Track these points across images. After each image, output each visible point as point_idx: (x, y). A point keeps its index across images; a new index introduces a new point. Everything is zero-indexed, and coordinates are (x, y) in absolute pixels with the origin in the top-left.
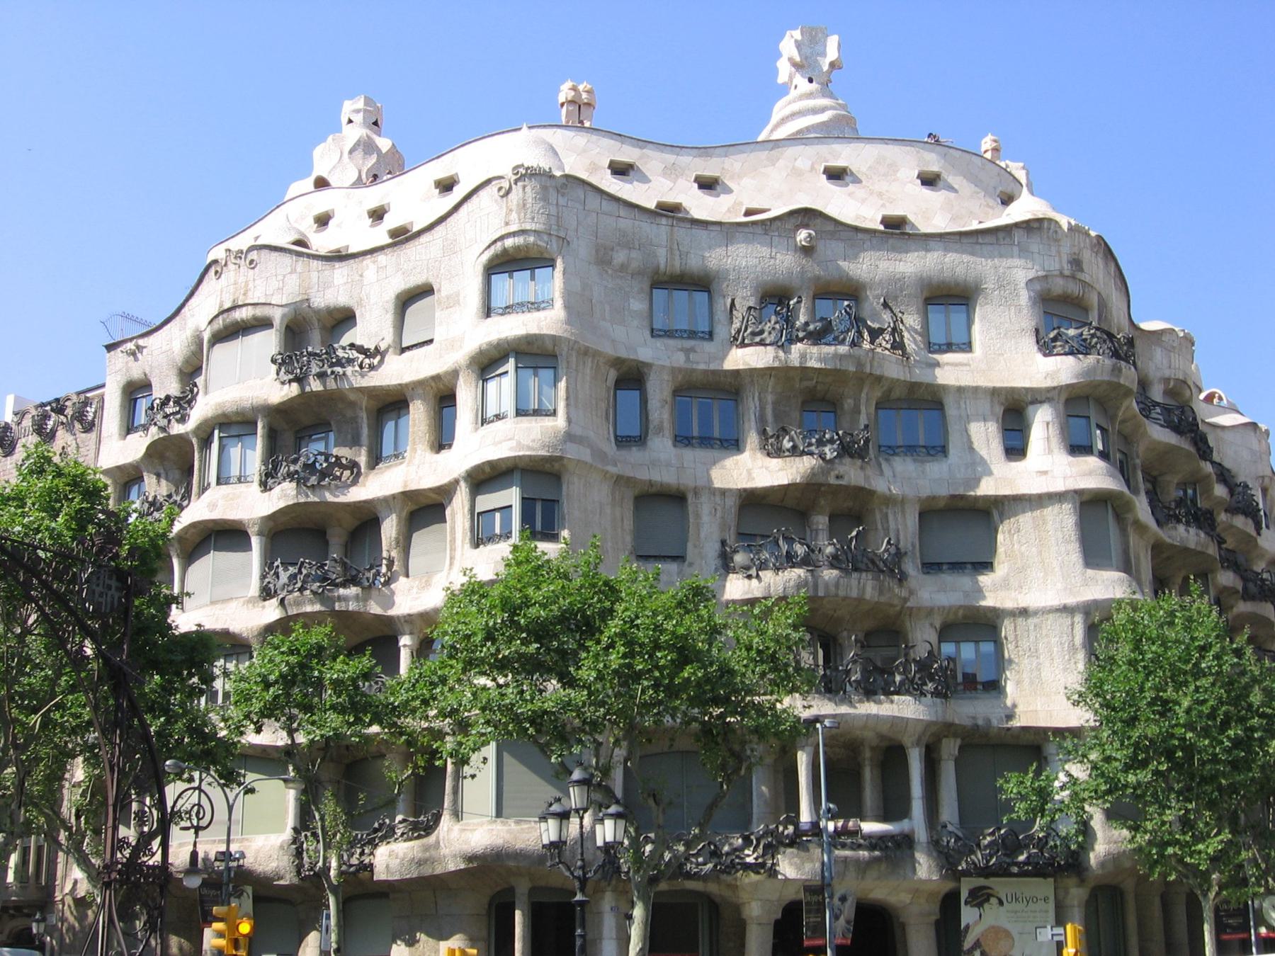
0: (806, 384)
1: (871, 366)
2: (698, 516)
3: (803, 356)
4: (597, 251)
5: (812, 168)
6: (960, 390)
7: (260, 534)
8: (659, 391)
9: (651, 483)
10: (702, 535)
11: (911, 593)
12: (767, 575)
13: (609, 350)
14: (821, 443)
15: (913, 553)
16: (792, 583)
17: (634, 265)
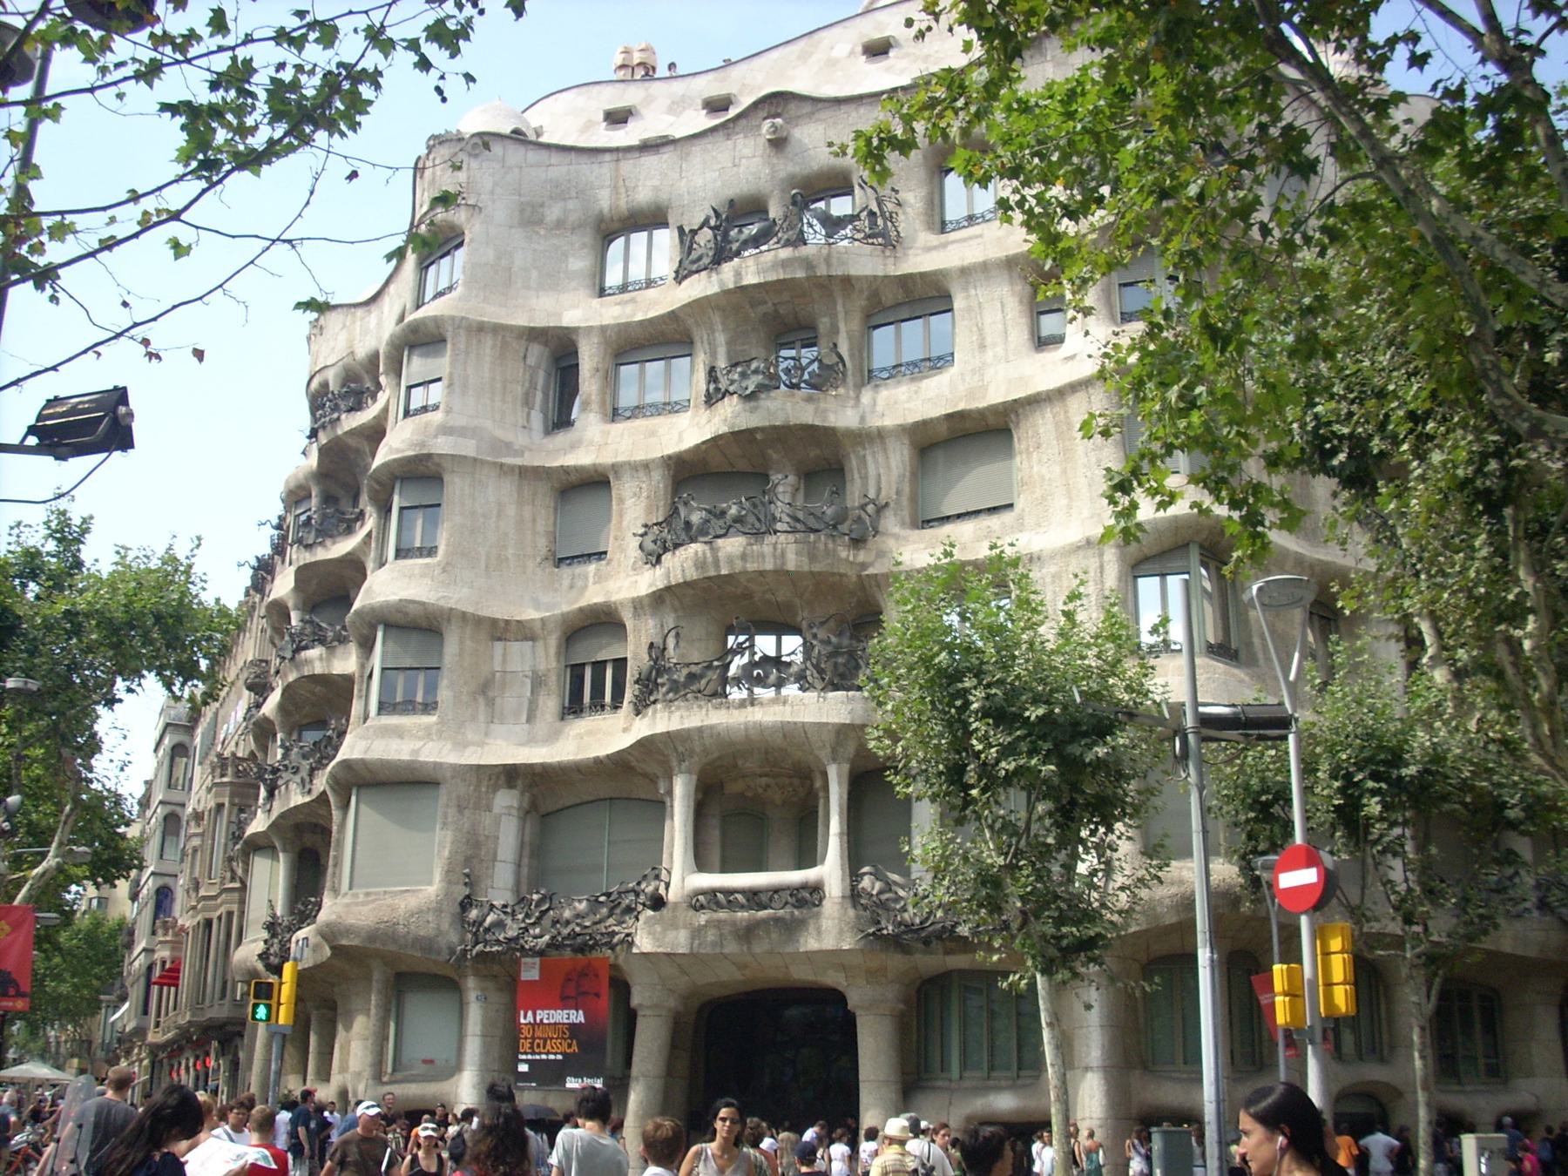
0: (762, 309)
1: (829, 265)
2: (621, 501)
3: (738, 274)
4: (522, 211)
5: (852, 53)
6: (965, 272)
7: (296, 608)
8: (589, 359)
9: (565, 470)
10: (625, 523)
11: (881, 554)
12: (666, 558)
13: (521, 320)
14: (744, 375)
15: (898, 502)
16: (690, 563)
17: (573, 217)
